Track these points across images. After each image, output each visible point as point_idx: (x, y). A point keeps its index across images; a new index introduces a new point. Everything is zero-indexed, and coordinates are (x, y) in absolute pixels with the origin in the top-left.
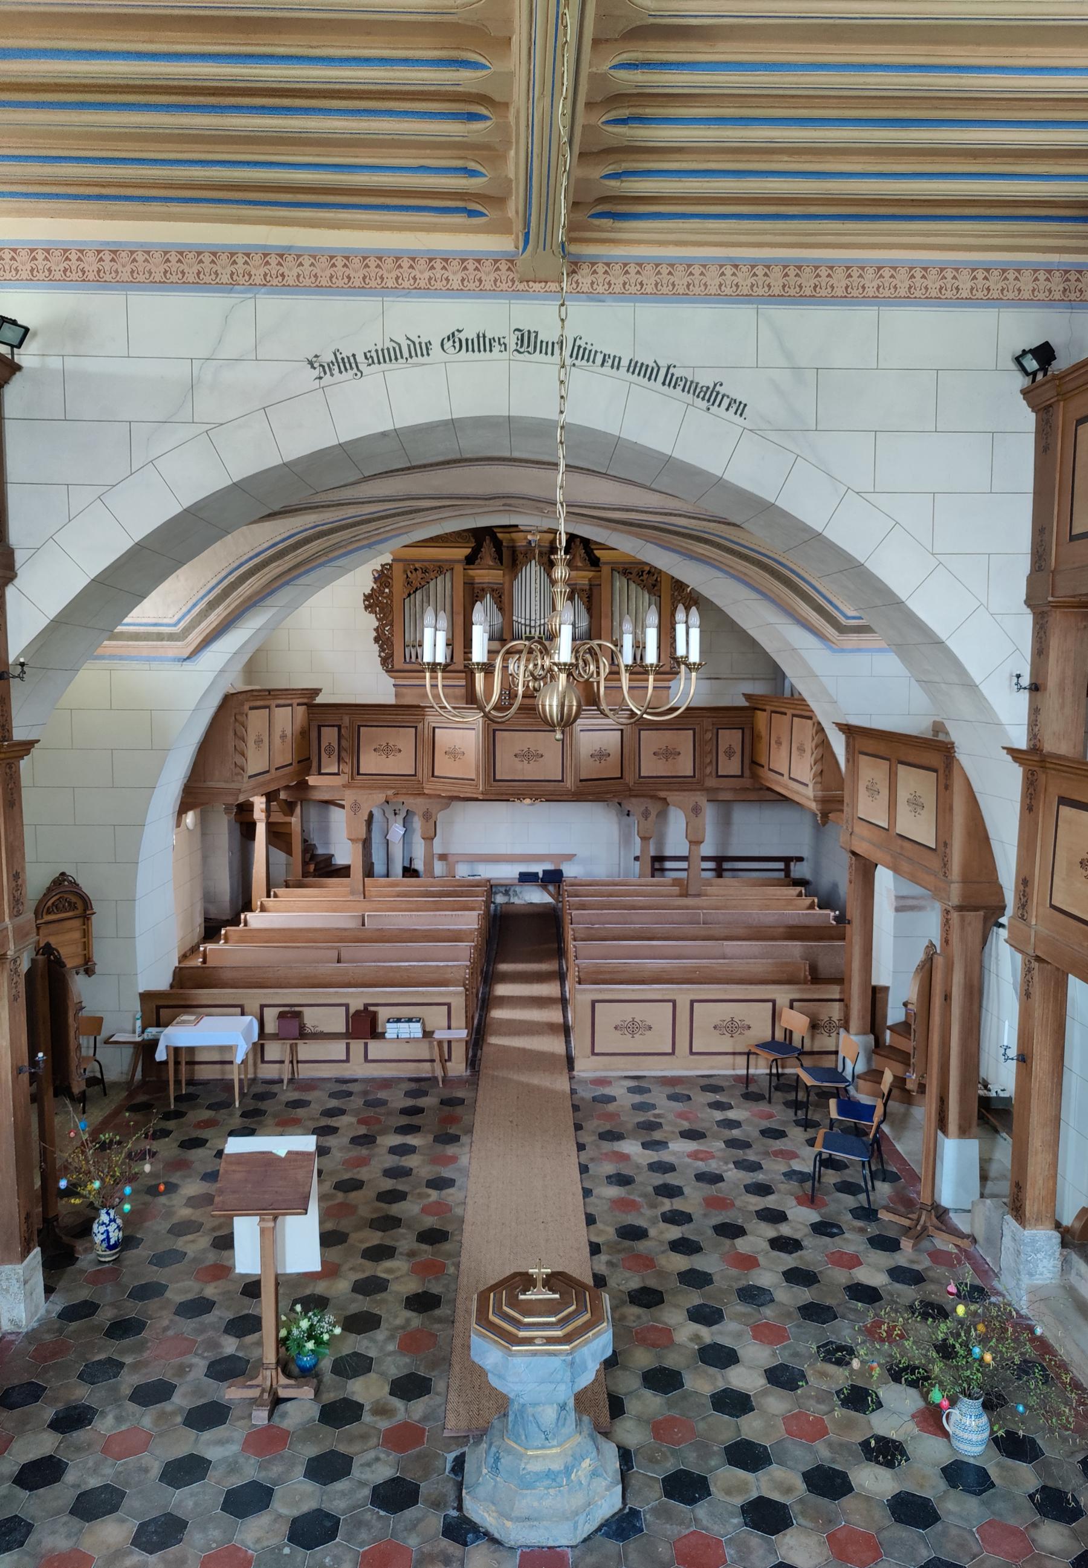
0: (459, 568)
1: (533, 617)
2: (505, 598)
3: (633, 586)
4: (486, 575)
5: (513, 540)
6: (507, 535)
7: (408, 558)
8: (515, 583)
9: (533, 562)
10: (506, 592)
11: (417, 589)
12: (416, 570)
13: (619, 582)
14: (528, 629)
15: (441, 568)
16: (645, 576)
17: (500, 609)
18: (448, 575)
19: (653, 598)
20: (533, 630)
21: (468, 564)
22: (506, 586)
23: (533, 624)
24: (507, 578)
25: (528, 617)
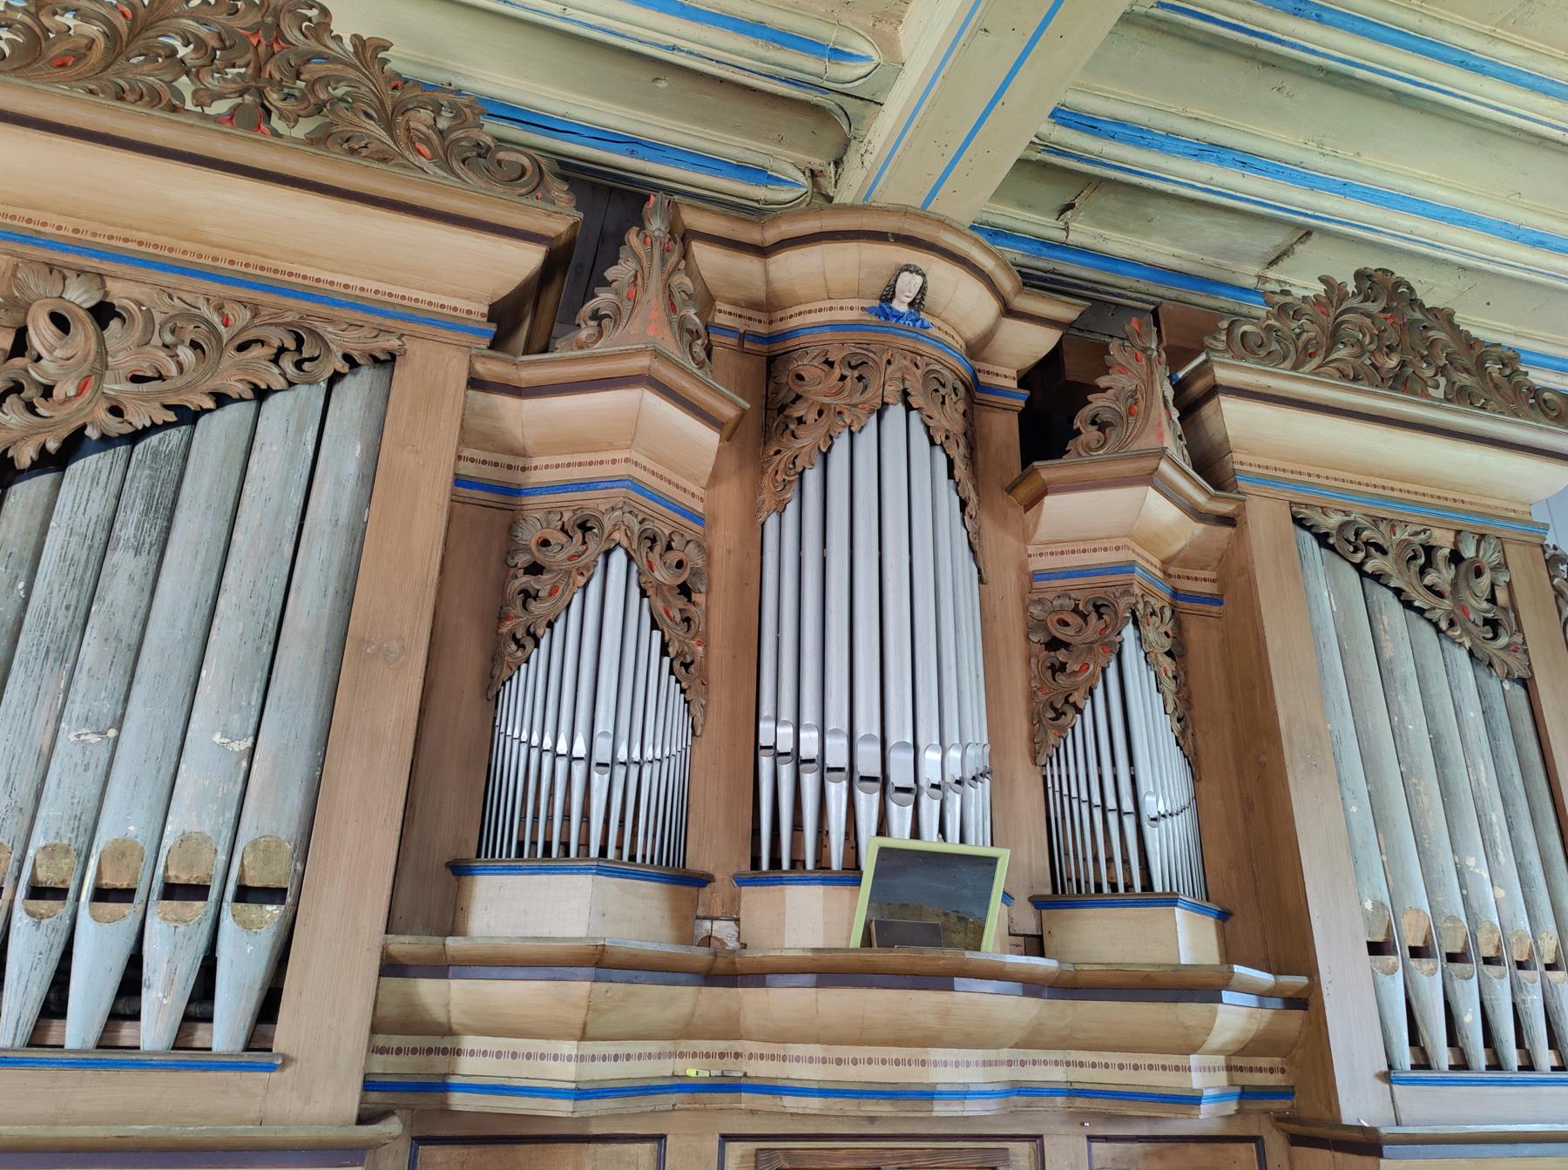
0: (437, 366)
1: (899, 732)
2: (718, 608)
3: (1393, 613)
4: (622, 426)
5: (770, 305)
6: (748, 266)
7: (54, 224)
8: (779, 533)
9: (896, 413)
10: (723, 573)
11: (75, 445)
12: (103, 313)
13: (1329, 588)
14: (868, 803)
15: (306, 342)
16: (1442, 576)
17: (683, 667)
18: (354, 394)
19: (1493, 686)
20: (900, 817)
21: (498, 343)
22: (725, 538)
23: (900, 775)
24: (730, 497)
25: (867, 724)
